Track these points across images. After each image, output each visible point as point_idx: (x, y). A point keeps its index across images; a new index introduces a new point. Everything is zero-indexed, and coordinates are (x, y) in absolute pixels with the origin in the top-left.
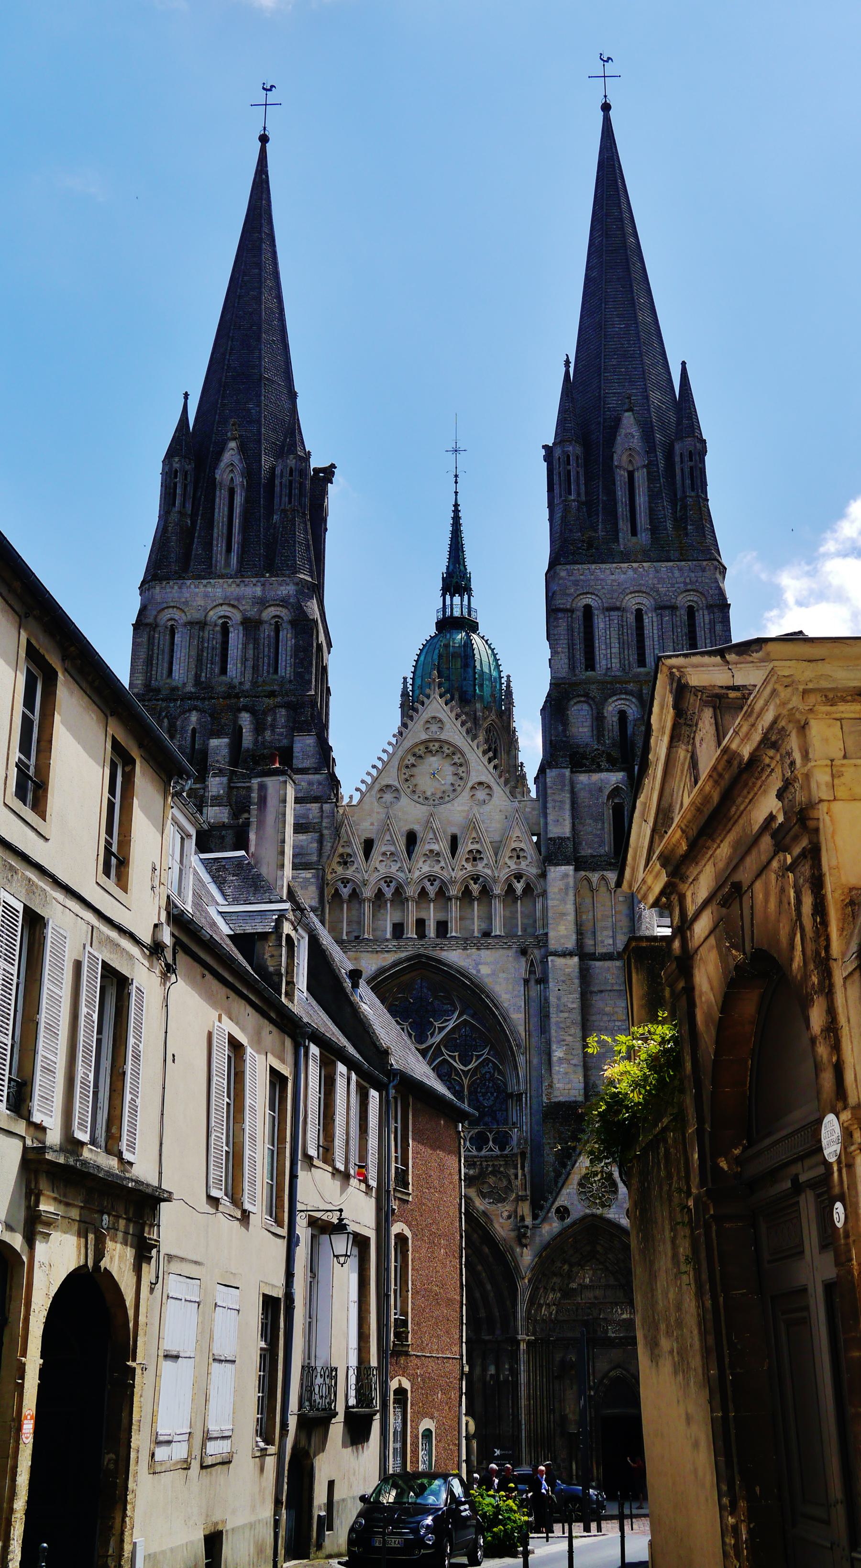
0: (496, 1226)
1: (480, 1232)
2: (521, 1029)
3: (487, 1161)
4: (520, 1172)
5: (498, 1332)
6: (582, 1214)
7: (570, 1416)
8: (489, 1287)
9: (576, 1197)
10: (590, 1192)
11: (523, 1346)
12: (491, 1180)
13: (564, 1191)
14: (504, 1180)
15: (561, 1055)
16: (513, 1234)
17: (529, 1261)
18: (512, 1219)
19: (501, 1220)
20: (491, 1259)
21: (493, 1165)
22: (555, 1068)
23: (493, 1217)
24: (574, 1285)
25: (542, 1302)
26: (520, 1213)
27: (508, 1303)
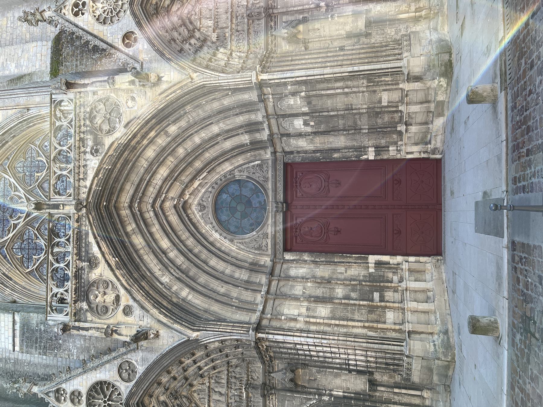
0: (140, 113)
1: (152, 134)
2: (10, 112)
3: (80, 127)
4: (89, 88)
5: (259, 117)
6: (131, 18)
7: (348, 28)
8: (215, 129)
9: (115, 26)
10: (112, 12)
11: (264, 77)
12: (98, 120)
13: (109, 41)
14: (99, 107)
15: (14, 65)
16: (150, 93)
17: (176, 73)
18: (135, 95)
19: (136, 108)
20: (183, 123)
21: (84, 120)
22: (24, 70)
23: (132, 117)
24: (214, 37)
25: (222, 63)
26: (126, 86)
27: (227, 102)
